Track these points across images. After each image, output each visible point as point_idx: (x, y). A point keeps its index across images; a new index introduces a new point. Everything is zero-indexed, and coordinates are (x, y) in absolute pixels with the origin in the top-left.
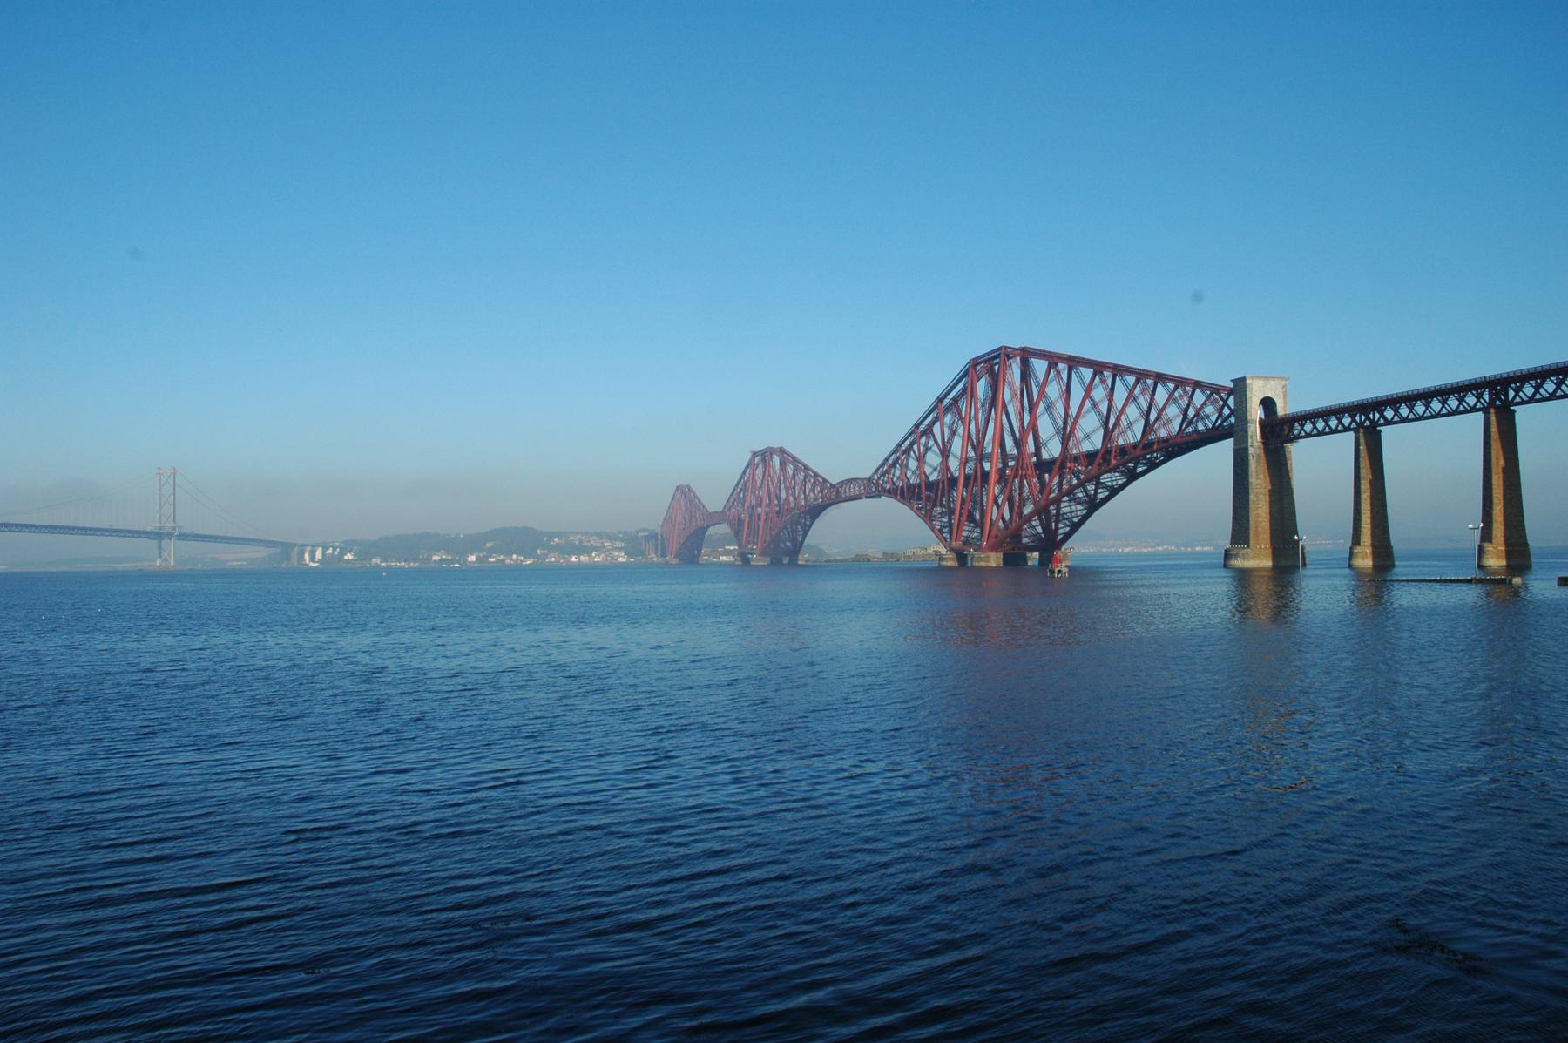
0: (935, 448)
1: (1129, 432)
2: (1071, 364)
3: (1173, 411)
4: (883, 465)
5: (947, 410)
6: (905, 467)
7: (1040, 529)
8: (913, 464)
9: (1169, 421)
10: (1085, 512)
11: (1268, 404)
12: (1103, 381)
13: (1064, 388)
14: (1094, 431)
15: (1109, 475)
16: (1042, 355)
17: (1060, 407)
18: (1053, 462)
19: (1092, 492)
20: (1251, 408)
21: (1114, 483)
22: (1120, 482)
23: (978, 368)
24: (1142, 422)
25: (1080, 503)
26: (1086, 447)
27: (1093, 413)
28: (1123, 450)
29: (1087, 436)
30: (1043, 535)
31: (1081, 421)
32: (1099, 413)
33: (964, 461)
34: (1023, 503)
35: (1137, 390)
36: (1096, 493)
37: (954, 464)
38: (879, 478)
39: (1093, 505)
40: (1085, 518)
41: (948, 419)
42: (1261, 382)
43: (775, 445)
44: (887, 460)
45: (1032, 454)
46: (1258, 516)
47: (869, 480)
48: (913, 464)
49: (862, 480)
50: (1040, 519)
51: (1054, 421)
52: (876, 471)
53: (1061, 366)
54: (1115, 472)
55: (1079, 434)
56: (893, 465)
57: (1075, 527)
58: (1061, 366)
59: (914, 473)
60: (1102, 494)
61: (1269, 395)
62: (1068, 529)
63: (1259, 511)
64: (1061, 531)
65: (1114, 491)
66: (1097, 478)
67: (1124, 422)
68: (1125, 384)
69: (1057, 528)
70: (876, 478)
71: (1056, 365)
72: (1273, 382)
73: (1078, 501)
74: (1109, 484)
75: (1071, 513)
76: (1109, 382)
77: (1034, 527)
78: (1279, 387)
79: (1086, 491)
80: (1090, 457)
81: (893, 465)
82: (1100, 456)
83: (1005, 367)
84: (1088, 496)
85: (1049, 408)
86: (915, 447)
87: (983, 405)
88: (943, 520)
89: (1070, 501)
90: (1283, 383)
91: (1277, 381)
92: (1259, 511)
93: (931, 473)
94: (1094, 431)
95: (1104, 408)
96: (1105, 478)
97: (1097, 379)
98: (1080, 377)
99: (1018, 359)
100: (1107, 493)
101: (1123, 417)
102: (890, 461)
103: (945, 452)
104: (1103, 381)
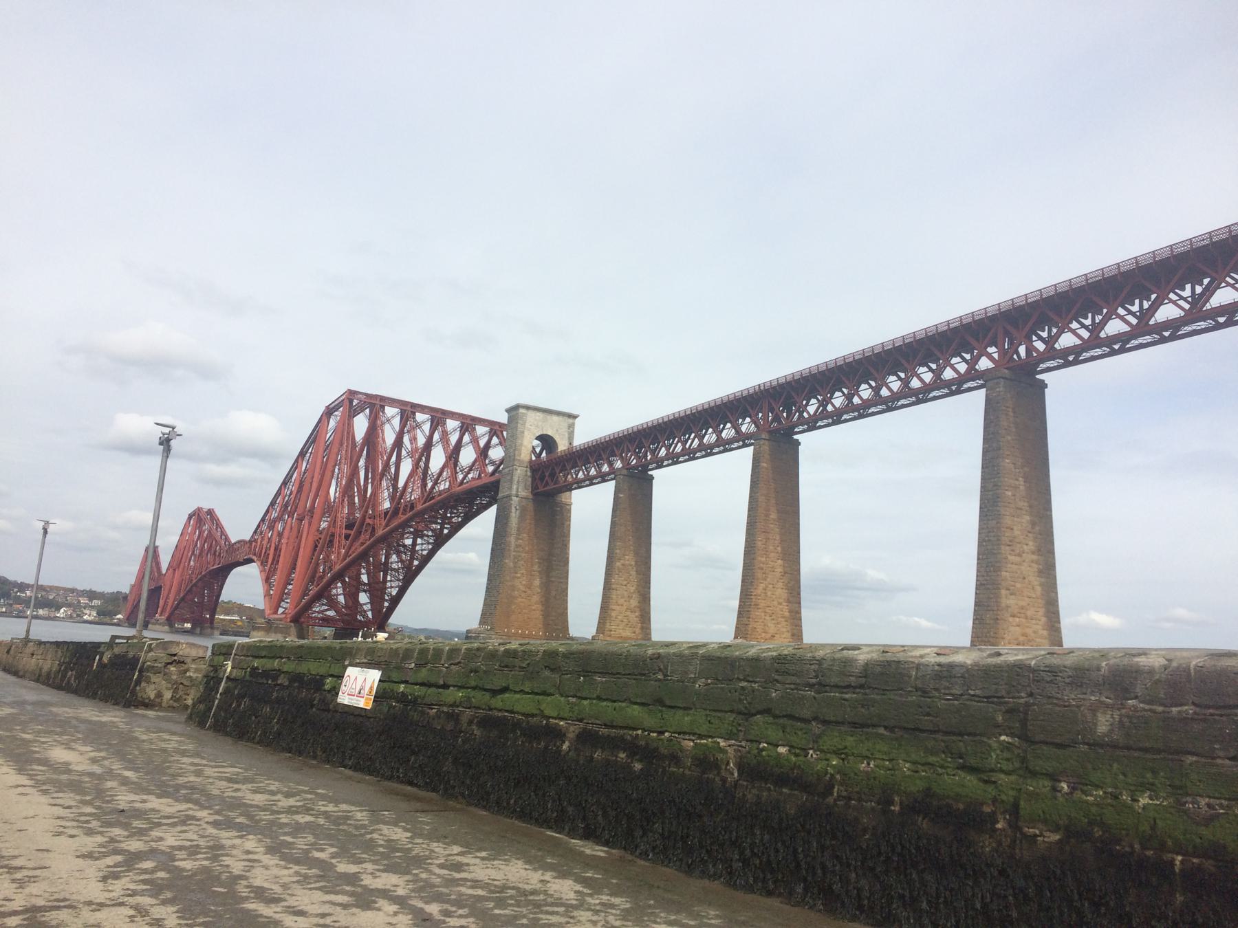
11: (547, 442)
20: (521, 445)
39: (410, 575)
42: (540, 415)
43: (206, 506)
46: (513, 588)
47: (250, 542)
57: (395, 601)
60: (416, 563)
61: (549, 434)
63: (517, 583)
65: (426, 560)
72: (555, 418)
78: (566, 425)
90: (571, 421)
91: (561, 418)
92: (517, 583)
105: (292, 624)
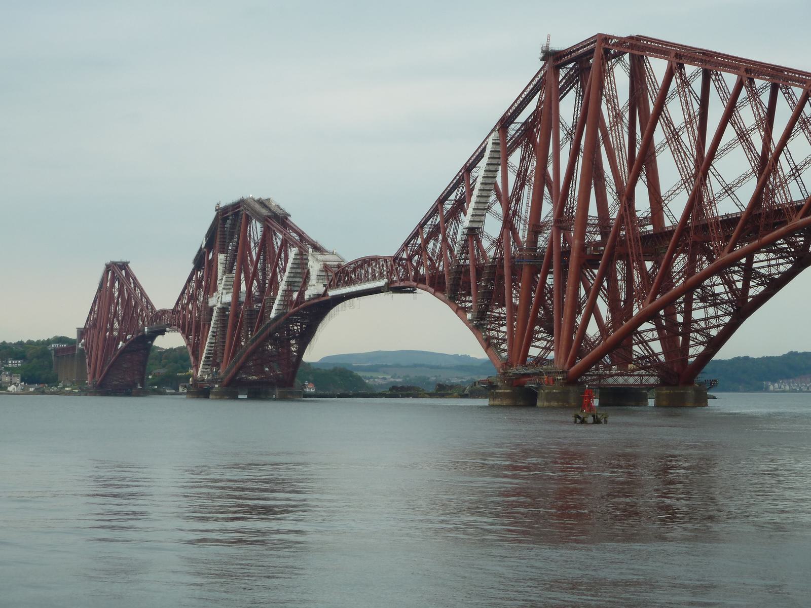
0: (498, 208)
1: (793, 185)
2: (708, 67)
4: (415, 234)
5: (516, 144)
7: (657, 347)
10: (727, 319)
12: (754, 95)
13: (696, 107)
14: (740, 182)
15: (762, 256)
16: (661, 49)
17: (686, 139)
18: (671, 233)
19: (739, 285)
21: (773, 270)
22: (782, 269)
23: (562, 73)
25: (715, 305)
26: (725, 208)
27: (739, 149)
28: (781, 215)
29: (728, 190)
30: (662, 358)
31: (716, 164)
32: (750, 147)
33: (536, 228)
34: (629, 302)
36: (746, 287)
37: (523, 233)
38: (410, 258)
40: (729, 331)
41: (515, 159)
44: (422, 225)
45: (645, 218)
49: (385, 260)
50: (659, 328)
51: (680, 164)
52: (406, 244)
53: (690, 69)
54: (769, 252)
55: (714, 185)
56: (433, 235)
57: (715, 344)
58: (690, 69)
60: (755, 290)
62: (701, 349)
64: (692, 351)
65: (775, 285)
66: (750, 255)
67: (784, 166)
68: (789, 96)
69: (686, 346)
70: (405, 256)
71: (681, 66)
73: (711, 300)
74: (762, 271)
75: (706, 319)
76: (765, 98)
77: (644, 342)
79: (729, 283)
80: (729, 222)
81: (433, 235)
82: (741, 222)
83: (604, 73)
84: (732, 291)
85: (674, 136)
87: (569, 135)
88: (504, 329)
89: (703, 299)
93: (490, 249)
94: (740, 182)
95: (757, 140)
96: (761, 261)
97: (744, 93)
98: (721, 88)
99: (627, 57)
100: (762, 288)
101: (782, 158)
102: (426, 229)
104: (754, 95)
105: (571, 388)
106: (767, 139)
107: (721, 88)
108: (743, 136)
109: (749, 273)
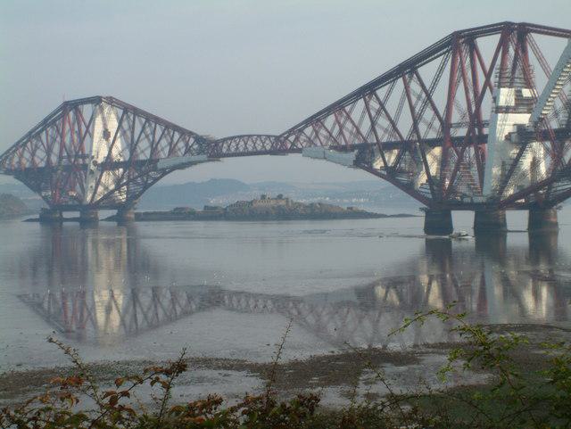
3: (181, 144)
4: (6, 153)
6: (21, 156)
8: (27, 155)
9: (179, 149)
12: (150, 125)
14: (145, 149)
24: (168, 148)
26: (142, 157)
29: (142, 152)
32: (149, 140)
35: (166, 132)
48: (27, 155)
59: (28, 161)
65: (156, 180)
67: (159, 148)
73: (138, 184)
79: (142, 179)
86: (29, 144)
95: (151, 137)
103: (49, 151)
104: (150, 125)
106: (154, 137)
107: (140, 121)
108: (147, 136)
109: (148, 176)
